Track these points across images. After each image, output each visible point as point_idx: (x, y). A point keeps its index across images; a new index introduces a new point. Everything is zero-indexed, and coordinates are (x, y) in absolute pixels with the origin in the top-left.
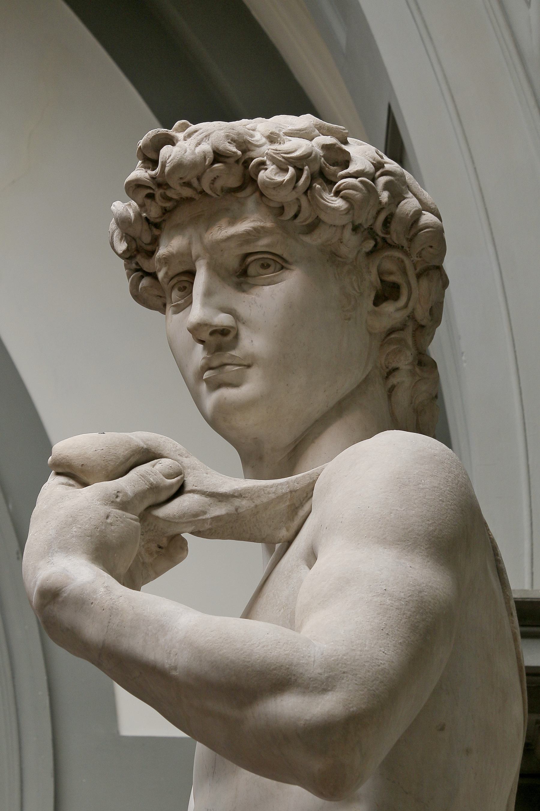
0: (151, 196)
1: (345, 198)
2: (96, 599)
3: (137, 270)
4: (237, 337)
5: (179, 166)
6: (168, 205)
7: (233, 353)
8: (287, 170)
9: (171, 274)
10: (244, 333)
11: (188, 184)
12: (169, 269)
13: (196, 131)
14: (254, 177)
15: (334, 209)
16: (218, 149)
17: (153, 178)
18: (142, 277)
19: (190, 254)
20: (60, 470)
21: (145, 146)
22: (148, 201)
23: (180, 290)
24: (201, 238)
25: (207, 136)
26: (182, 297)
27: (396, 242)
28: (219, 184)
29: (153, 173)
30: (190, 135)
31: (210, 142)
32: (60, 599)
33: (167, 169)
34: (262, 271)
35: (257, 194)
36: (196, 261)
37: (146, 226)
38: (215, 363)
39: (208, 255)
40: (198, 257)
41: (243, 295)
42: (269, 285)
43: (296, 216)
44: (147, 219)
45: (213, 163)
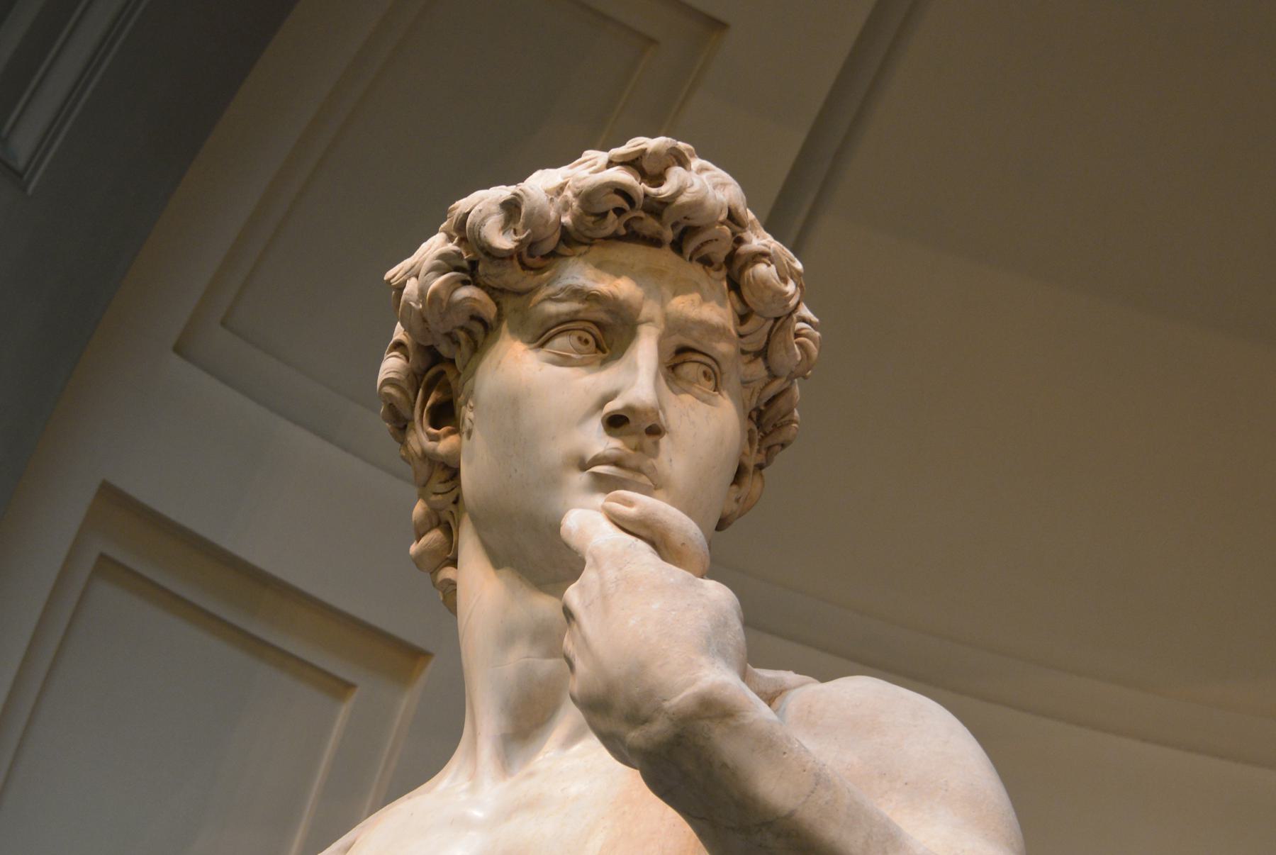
0: (619, 211)
1: (801, 345)
2: (791, 750)
3: (457, 269)
4: (656, 444)
5: (698, 205)
6: (623, 232)
7: (654, 461)
8: (785, 282)
9: (581, 315)
10: (664, 441)
11: (674, 226)
12: (586, 309)
13: (707, 170)
14: (738, 264)
15: (795, 354)
16: (736, 209)
17: (646, 195)
18: (465, 283)
19: (638, 311)
20: (643, 532)
21: (656, 154)
22: (612, 216)
23: (580, 339)
24: (663, 303)
25: (724, 185)
26: (579, 351)
27: (764, 420)
28: (707, 250)
29: (653, 190)
30: (701, 170)
31: (727, 192)
32: (732, 722)
33: (683, 199)
34: (703, 379)
35: (725, 284)
36: (642, 323)
37: (557, 236)
38: (633, 463)
39: (663, 326)
40: (649, 321)
41: (672, 396)
42: (704, 401)
43: (741, 336)
44: (564, 228)
45: (722, 223)
